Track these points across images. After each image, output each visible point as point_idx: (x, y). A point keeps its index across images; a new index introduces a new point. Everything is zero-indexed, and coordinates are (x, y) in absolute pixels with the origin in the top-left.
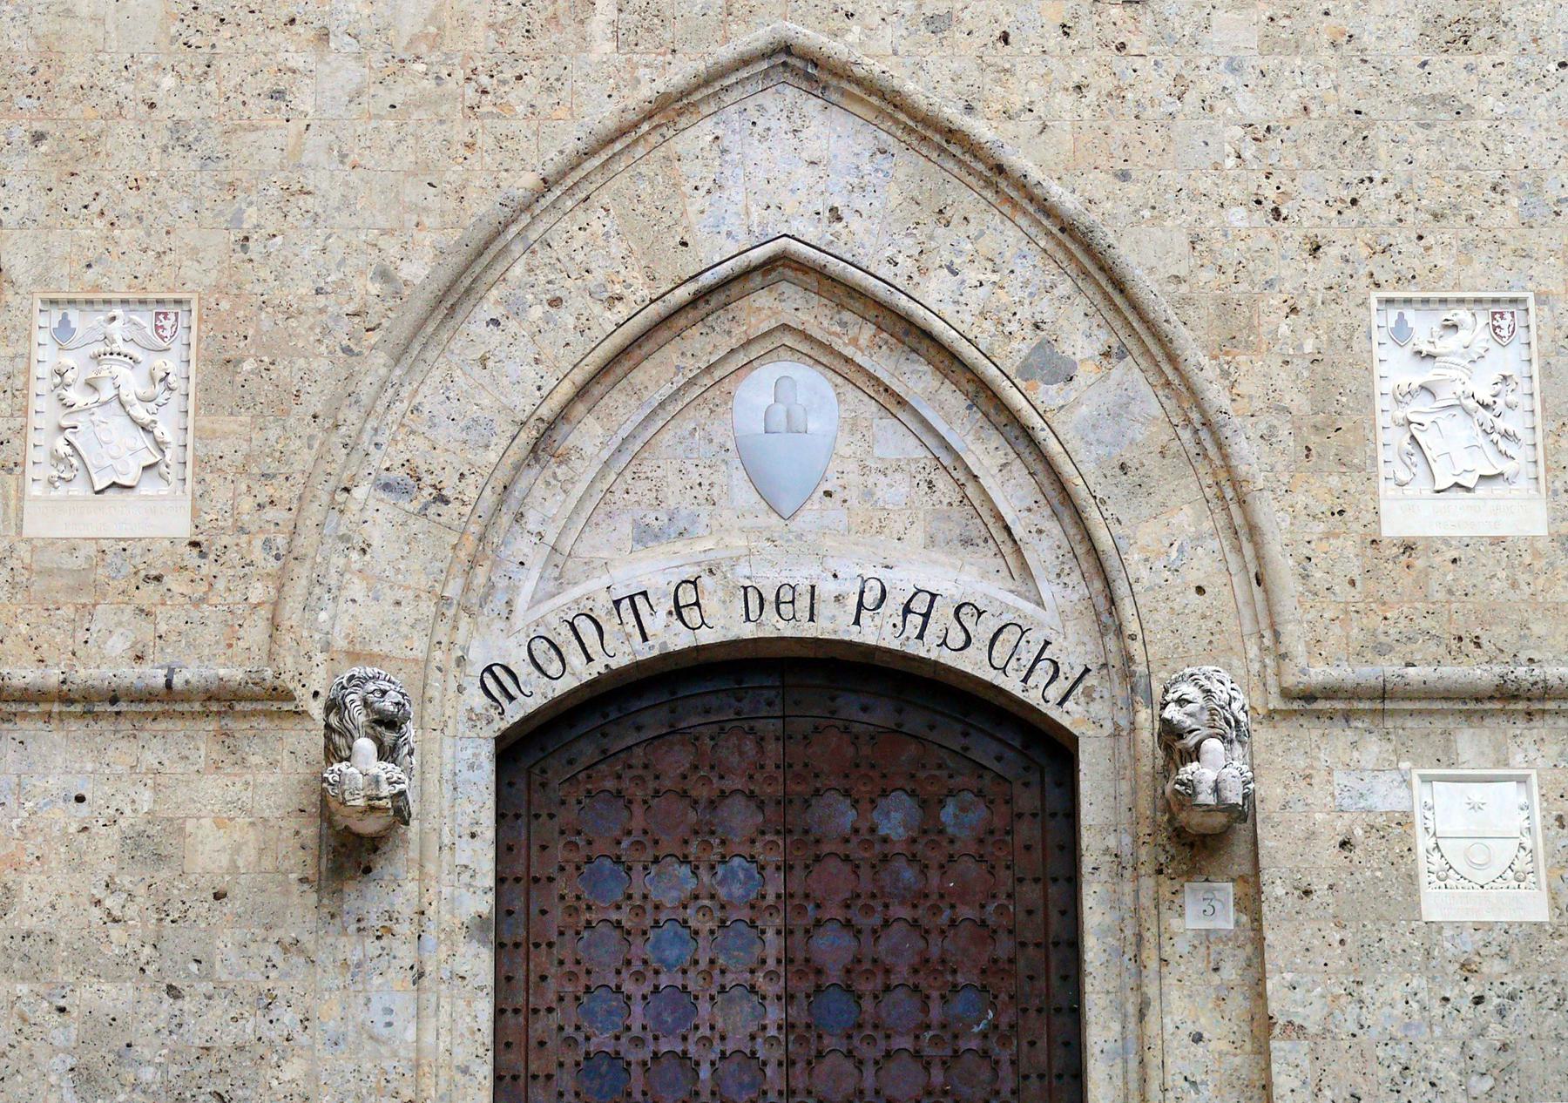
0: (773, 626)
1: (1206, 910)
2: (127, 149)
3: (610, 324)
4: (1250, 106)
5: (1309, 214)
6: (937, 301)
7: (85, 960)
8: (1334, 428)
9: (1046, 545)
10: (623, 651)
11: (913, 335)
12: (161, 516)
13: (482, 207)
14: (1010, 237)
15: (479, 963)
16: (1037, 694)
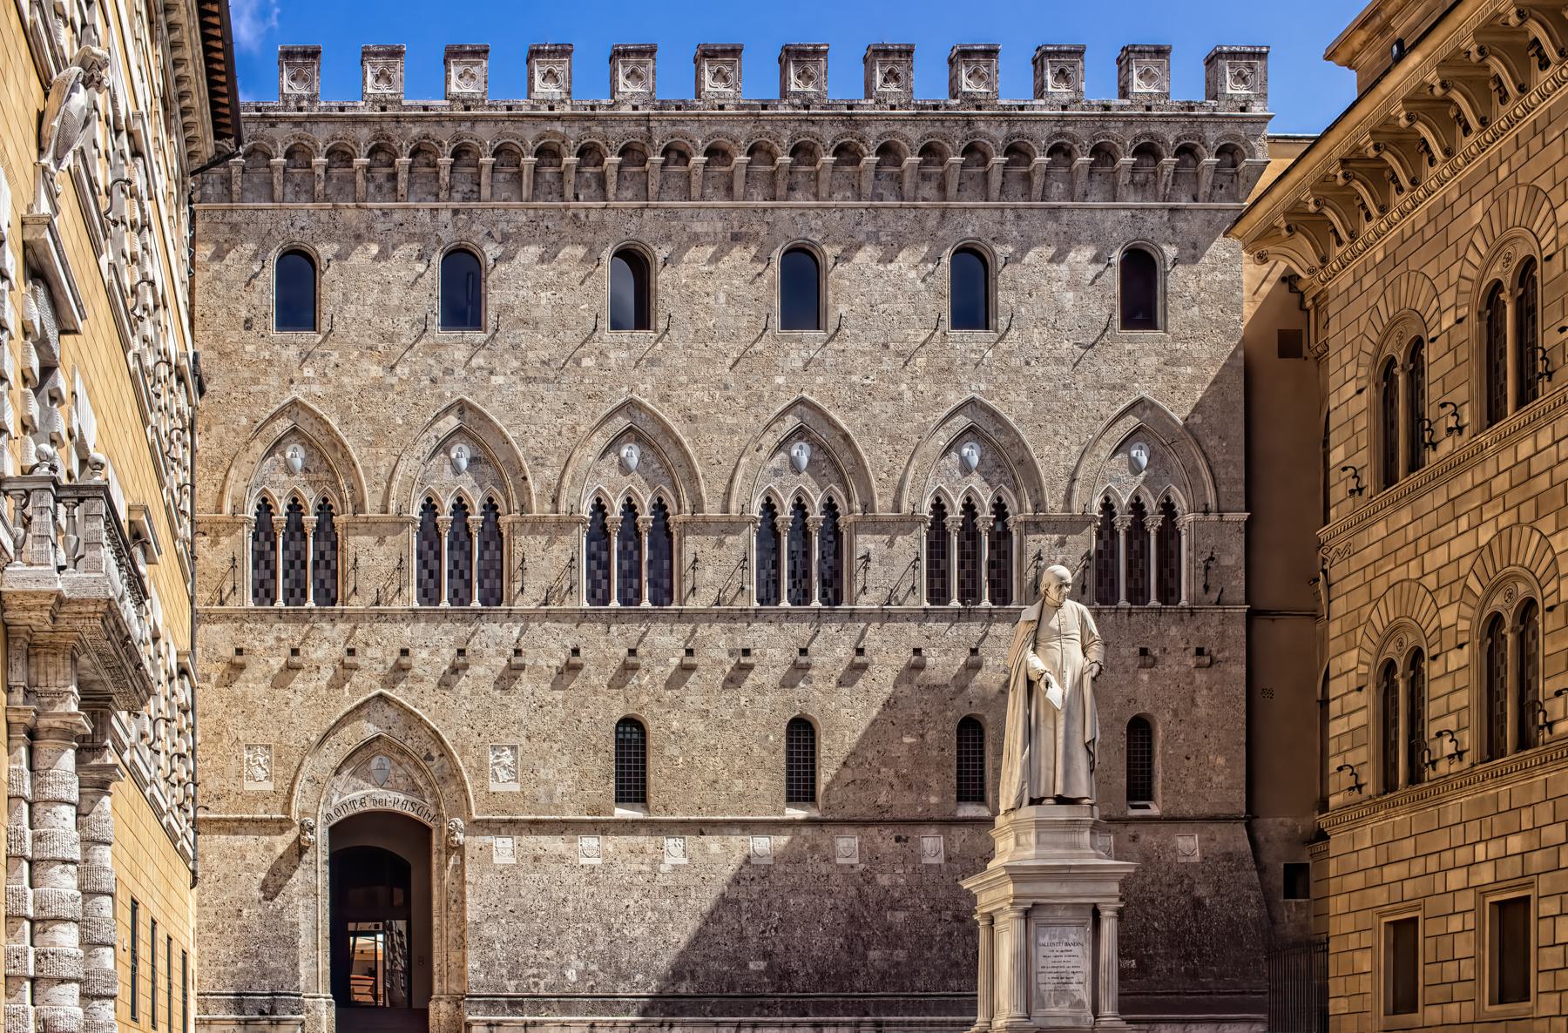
0: (379, 807)
2: (259, 716)
3: (350, 749)
4: (468, 706)
5: (479, 725)
7: (259, 868)
8: (480, 771)
10: (351, 812)
11: (403, 752)
12: (268, 786)
13: (325, 727)
15: (327, 869)
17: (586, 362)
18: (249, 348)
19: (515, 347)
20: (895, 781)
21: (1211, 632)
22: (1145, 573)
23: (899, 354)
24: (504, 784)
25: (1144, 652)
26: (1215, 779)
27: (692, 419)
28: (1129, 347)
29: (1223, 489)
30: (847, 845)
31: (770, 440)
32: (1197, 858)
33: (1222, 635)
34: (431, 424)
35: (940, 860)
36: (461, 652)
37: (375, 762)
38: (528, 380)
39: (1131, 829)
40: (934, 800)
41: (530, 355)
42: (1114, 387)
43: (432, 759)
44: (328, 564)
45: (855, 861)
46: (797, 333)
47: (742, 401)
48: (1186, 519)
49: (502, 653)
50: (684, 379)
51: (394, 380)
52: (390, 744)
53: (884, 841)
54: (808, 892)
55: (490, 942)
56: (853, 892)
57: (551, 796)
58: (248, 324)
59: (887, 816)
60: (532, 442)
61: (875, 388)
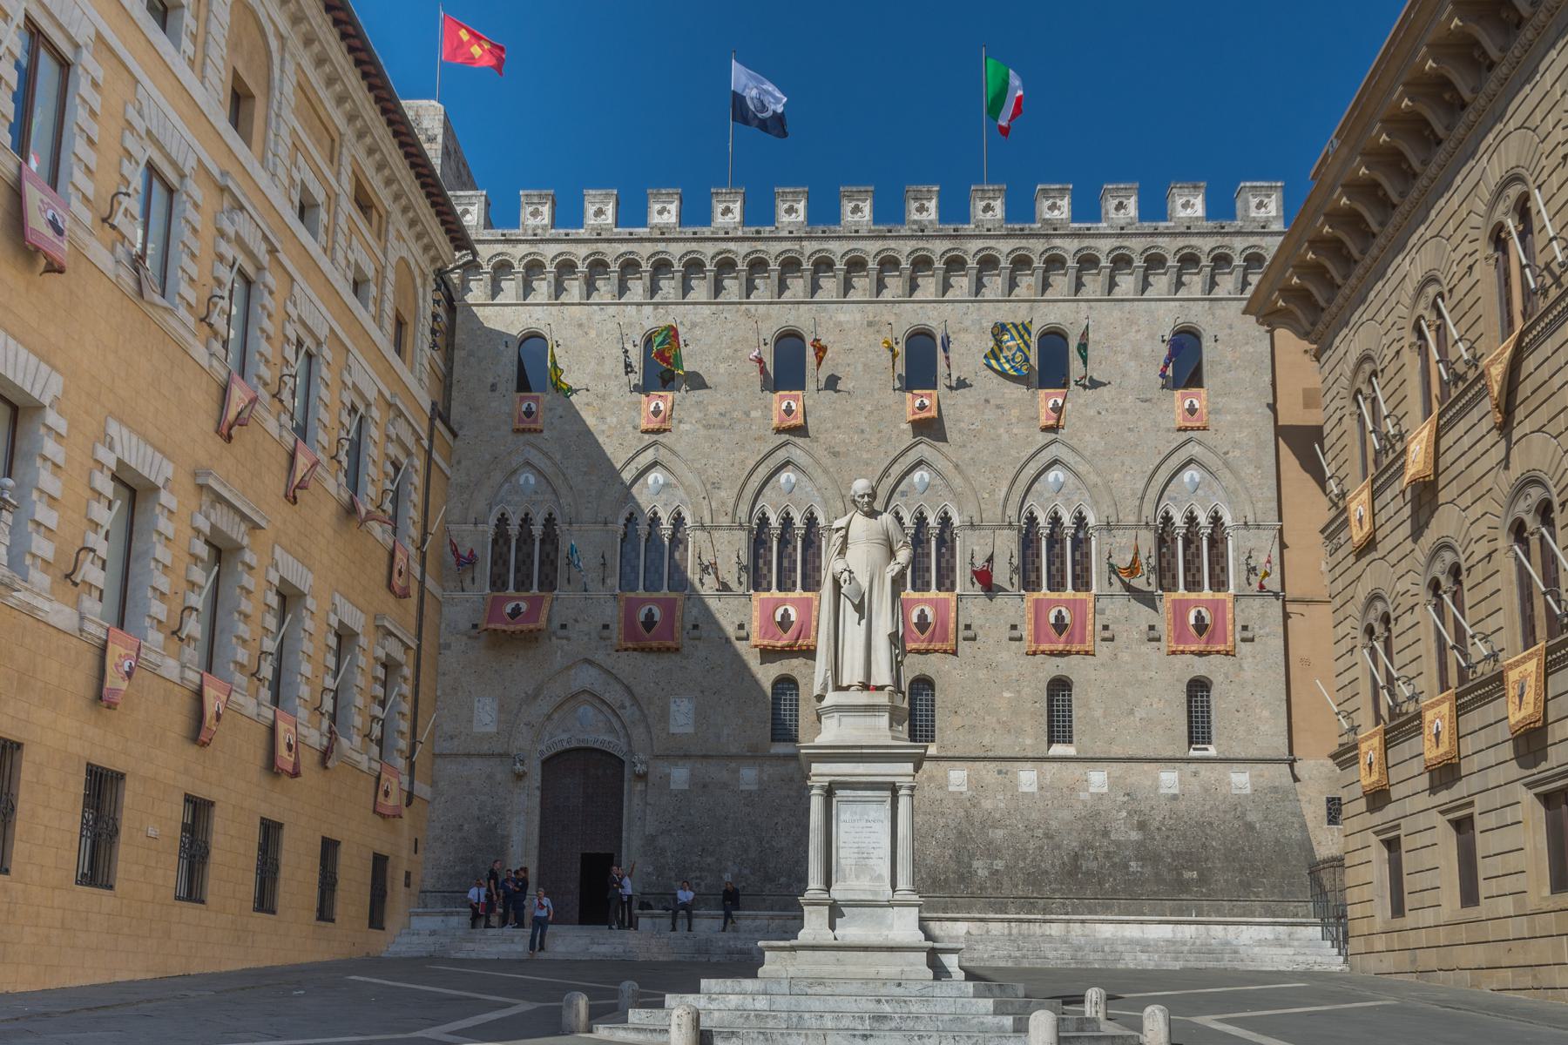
1: (640, 787)
6: (607, 697)
8: (664, 716)
9: (622, 734)
10: (560, 748)
11: (603, 702)
12: (492, 729)
14: (618, 687)
16: (620, 755)
17: (754, 414)
18: (493, 405)
19: (699, 403)
20: (997, 727)
21: (1255, 614)
22: (1199, 570)
23: (998, 407)
26: (1262, 728)
27: (836, 454)
30: (958, 777)
31: (897, 470)
32: (1248, 791)
33: (1263, 616)
34: (633, 458)
35: (1034, 789)
37: (581, 710)
38: (708, 427)
39: (1193, 767)
40: (1029, 741)
41: (711, 409)
43: (624, 707)
44: (549, 562)
45: (964, 789)
47: (874, 441)
50: (829, 425)
51: (604, 427)
53: (988, 771)
54: (925, 813)
56: (961, 813)
58: (493, 388)
59: (990, 754)
60: (710, 472)
61: (980, 432)
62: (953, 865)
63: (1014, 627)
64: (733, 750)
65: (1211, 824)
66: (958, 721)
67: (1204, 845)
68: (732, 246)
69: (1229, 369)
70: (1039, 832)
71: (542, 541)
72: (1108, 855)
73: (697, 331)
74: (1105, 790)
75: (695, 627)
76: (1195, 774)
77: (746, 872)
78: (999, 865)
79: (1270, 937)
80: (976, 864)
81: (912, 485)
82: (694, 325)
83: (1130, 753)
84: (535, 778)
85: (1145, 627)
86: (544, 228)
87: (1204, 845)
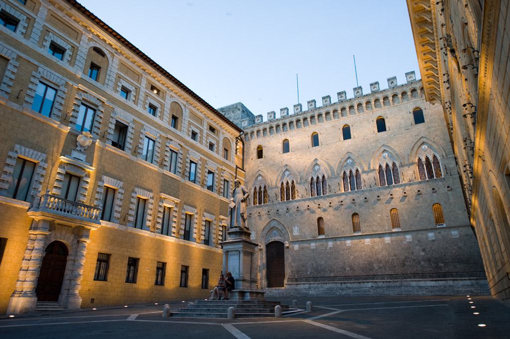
1: (288, 250)
6: (279, 228)
11: (278, 229)
24: (296, 232)
25: (433, 189)
26: (459, 216)
28: (418, 127)
29: (447, 151)
30: (367, 241)
32: (458, 237)
35: (390, 242)
36: (288, 209)
38: (297, 159)
39: (438, 231)
40: (387, 228)
42: (415, 136)
43: (283, 230)
45: (369, 244)
46: (346, 140)
47: (336, 154)
48: (439, 158)
49: (295, 208)
52: (276, 228)
53: (377, 240)
55: (293, 266)
56: (369, 251)
57: (305, 235)
62: (368, 266)
63: (378, 197)
64: (309, 239)
65: (446, 248)
66: (366, 224)
67: (445, 255)
68: (299, 117)
69: (431, 116)
70: (392, 255)
71: (264, 192)
72: (414, 260)
73: (294, 138)
74: (411, 240)
75: (298, 208)
76: (440, 233)
77: (313, 271)
78: (381, 265)
79: (469, 284)
80: (374, 265)
81: (347, 164)
82: (293, 136)
83: (418, 228)
84: (264, 250)
85: (417, 191)
86: (260, 123)
87: (445, 255)
